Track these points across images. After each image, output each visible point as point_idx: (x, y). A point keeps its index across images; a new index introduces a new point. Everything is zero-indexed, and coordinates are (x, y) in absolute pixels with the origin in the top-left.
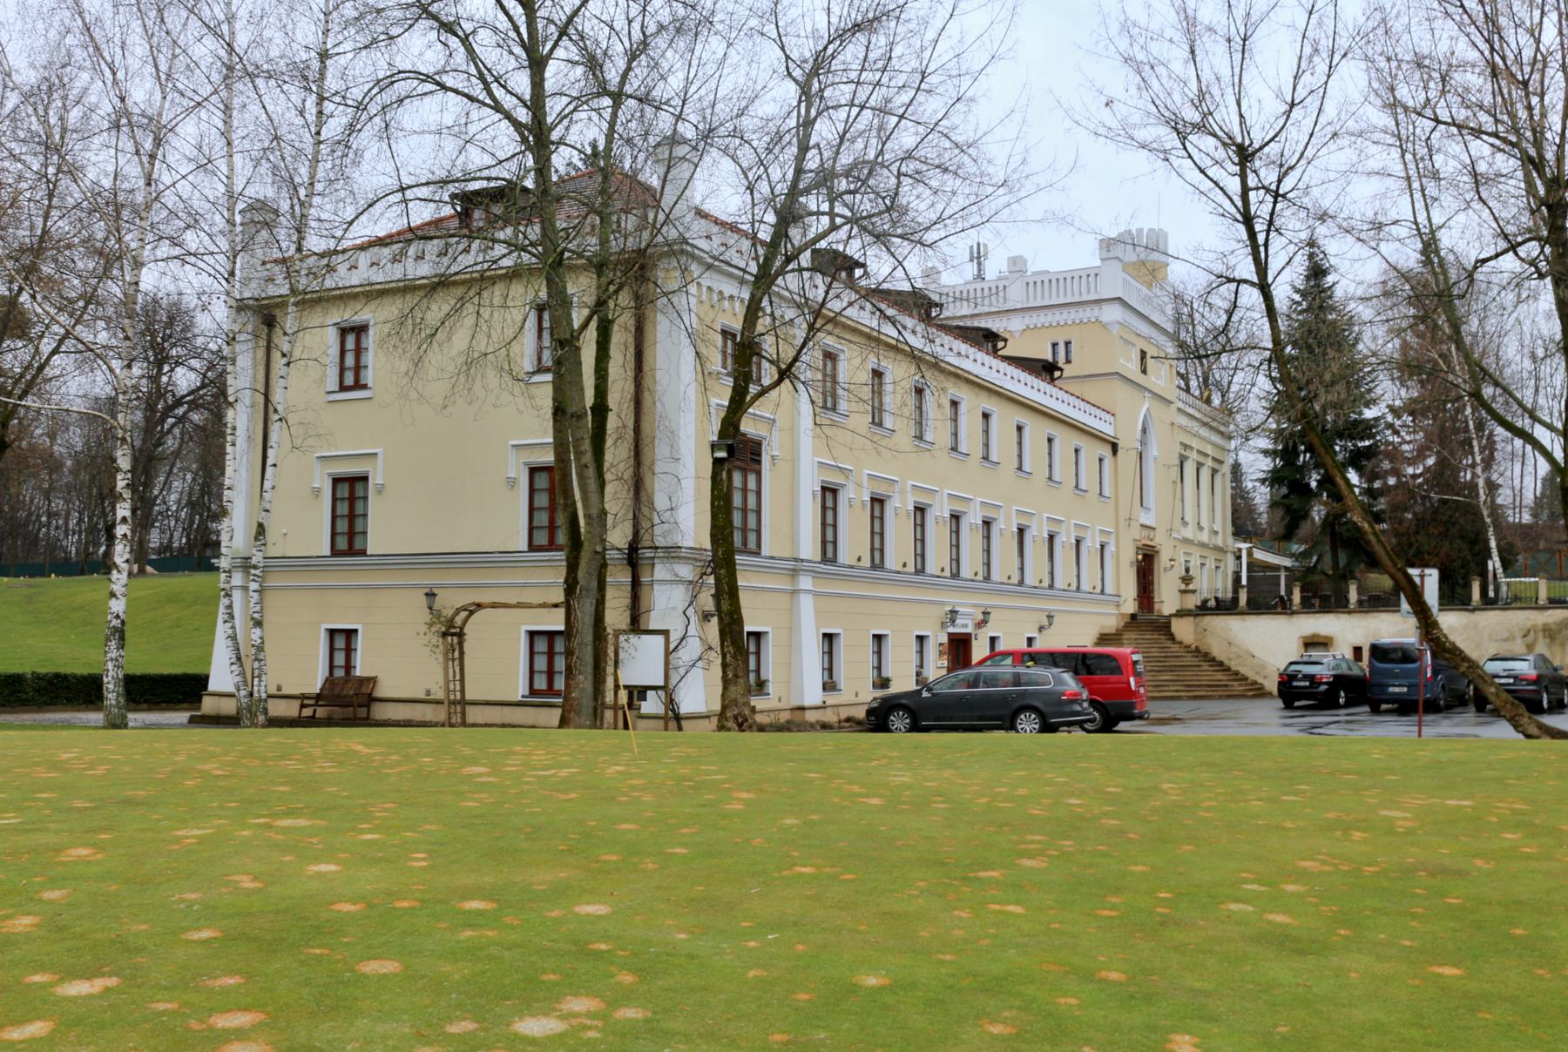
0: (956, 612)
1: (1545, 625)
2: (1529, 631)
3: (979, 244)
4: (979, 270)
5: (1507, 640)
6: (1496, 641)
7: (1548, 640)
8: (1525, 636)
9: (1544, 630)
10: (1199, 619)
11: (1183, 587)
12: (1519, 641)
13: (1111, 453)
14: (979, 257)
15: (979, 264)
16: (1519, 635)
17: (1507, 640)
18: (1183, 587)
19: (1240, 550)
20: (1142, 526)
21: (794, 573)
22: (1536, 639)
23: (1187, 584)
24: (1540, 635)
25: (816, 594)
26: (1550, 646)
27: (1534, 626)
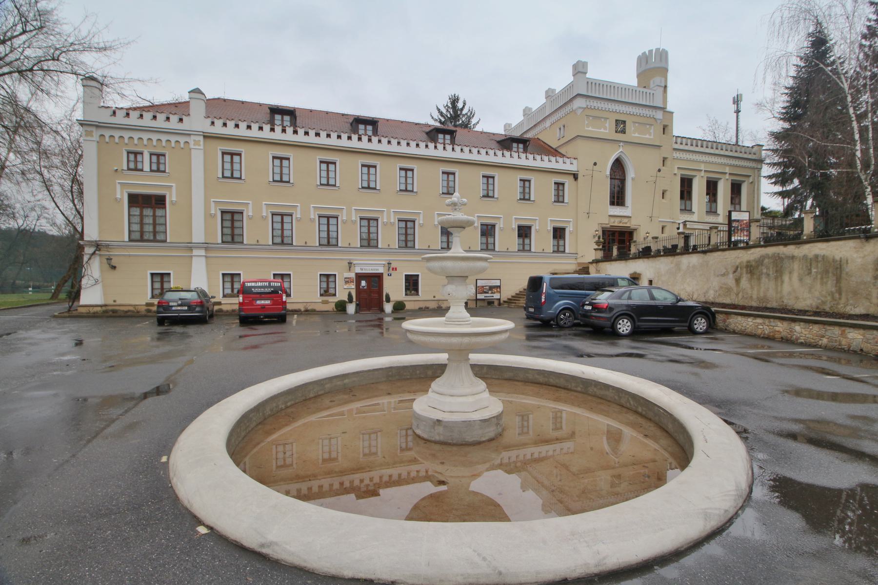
0: (351, 263)
1: (748, 262)
2: (737, 267)
3: (738, 95)
4: (738, 107)
5: (723, 275)
6: (718, 276)
7: (749, 275)
8: (735, 272)
9: (747, 267)
10: (598, 264)
11: (596, 247)
12: (731, 276)
13: (573, 179)
14: (738, 101)
15: (738, 105)
16: (731, 271)
17: (723, 275)
18: (596, 247)
19: (679, 224)
20: (610, 216)
21: (191, 249)
22: (741, 274)
23: (599, 245)
24: (745, 269)
25: (206, 257)
26: (750, 280)
27: (740, 263)
